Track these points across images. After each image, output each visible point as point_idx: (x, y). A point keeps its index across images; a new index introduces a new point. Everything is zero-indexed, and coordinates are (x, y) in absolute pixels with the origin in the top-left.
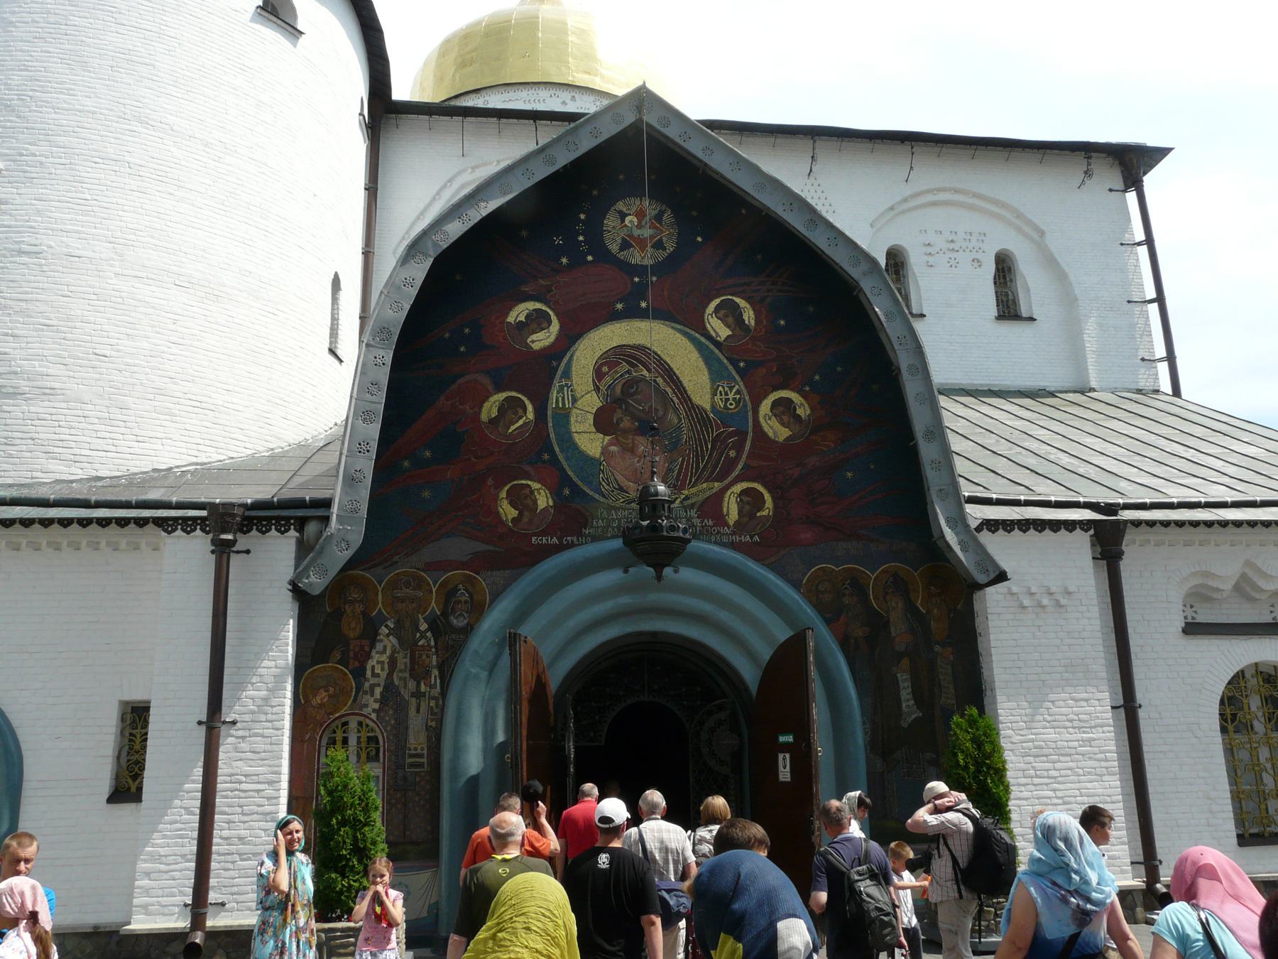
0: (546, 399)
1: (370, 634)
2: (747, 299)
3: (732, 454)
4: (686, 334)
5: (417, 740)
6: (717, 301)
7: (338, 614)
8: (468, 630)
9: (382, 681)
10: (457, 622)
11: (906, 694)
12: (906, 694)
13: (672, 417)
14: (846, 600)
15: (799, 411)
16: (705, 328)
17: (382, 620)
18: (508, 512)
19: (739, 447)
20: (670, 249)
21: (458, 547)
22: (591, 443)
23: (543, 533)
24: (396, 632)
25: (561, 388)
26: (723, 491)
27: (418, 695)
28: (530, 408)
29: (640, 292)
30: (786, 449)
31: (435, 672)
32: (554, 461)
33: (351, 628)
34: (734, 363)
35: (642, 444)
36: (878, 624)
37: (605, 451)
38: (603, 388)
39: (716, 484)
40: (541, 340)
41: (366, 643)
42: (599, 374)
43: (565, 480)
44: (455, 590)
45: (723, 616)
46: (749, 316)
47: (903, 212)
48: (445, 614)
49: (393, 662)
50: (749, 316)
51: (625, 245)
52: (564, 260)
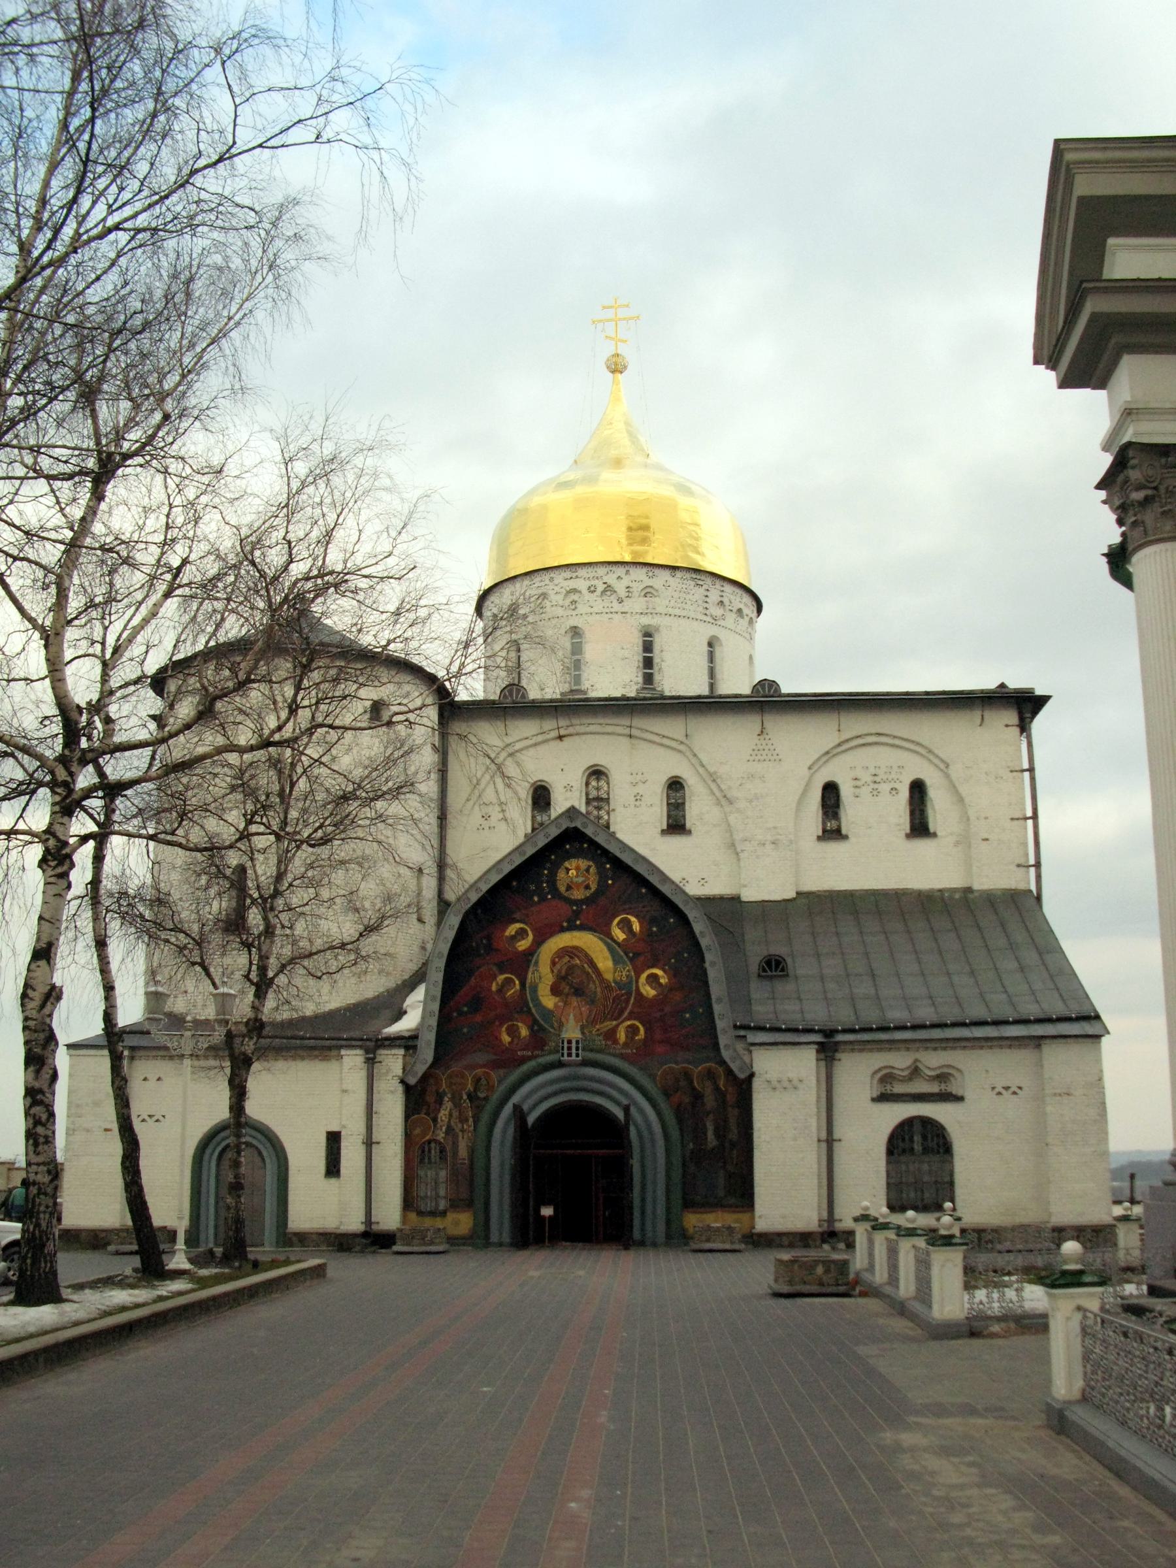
0: (525, 978)
1: (440, 1102)
2: (636, 917)
4: (601, 939)
5: (463, 1152)
7: (423, 1092)
8: (486, 1099)
10: (481, 1095)
11: (710, 1134)
12: (710, 1134)
13: (591, 985)
15: (662, 981)
17: (445, 1093)
18: (506, 1039)
19: (627, 1001)
20: (594, 887)
21: (481, 1058)
22: (549, 1002)
24: (452, 1099)
26: (618, 1026)
27: (463, 1131)
29: (577, 914)
30: (653, 1002)
31: (471, 1120)
33: (430, 1098)
34: (626, 954)
35: (574, 1001)
36: (697, 1097)
37: (556, 1005)
39: (614, 1023)
40: (523, 945)
42: (553, 963)
43: (535, 1021)
44: (479, 1080)
45: (614, 1093)
46: (636, 926)
48: (475, 1090)
49: (451, 1115)
50: (636, 926)
52: (536, 899)
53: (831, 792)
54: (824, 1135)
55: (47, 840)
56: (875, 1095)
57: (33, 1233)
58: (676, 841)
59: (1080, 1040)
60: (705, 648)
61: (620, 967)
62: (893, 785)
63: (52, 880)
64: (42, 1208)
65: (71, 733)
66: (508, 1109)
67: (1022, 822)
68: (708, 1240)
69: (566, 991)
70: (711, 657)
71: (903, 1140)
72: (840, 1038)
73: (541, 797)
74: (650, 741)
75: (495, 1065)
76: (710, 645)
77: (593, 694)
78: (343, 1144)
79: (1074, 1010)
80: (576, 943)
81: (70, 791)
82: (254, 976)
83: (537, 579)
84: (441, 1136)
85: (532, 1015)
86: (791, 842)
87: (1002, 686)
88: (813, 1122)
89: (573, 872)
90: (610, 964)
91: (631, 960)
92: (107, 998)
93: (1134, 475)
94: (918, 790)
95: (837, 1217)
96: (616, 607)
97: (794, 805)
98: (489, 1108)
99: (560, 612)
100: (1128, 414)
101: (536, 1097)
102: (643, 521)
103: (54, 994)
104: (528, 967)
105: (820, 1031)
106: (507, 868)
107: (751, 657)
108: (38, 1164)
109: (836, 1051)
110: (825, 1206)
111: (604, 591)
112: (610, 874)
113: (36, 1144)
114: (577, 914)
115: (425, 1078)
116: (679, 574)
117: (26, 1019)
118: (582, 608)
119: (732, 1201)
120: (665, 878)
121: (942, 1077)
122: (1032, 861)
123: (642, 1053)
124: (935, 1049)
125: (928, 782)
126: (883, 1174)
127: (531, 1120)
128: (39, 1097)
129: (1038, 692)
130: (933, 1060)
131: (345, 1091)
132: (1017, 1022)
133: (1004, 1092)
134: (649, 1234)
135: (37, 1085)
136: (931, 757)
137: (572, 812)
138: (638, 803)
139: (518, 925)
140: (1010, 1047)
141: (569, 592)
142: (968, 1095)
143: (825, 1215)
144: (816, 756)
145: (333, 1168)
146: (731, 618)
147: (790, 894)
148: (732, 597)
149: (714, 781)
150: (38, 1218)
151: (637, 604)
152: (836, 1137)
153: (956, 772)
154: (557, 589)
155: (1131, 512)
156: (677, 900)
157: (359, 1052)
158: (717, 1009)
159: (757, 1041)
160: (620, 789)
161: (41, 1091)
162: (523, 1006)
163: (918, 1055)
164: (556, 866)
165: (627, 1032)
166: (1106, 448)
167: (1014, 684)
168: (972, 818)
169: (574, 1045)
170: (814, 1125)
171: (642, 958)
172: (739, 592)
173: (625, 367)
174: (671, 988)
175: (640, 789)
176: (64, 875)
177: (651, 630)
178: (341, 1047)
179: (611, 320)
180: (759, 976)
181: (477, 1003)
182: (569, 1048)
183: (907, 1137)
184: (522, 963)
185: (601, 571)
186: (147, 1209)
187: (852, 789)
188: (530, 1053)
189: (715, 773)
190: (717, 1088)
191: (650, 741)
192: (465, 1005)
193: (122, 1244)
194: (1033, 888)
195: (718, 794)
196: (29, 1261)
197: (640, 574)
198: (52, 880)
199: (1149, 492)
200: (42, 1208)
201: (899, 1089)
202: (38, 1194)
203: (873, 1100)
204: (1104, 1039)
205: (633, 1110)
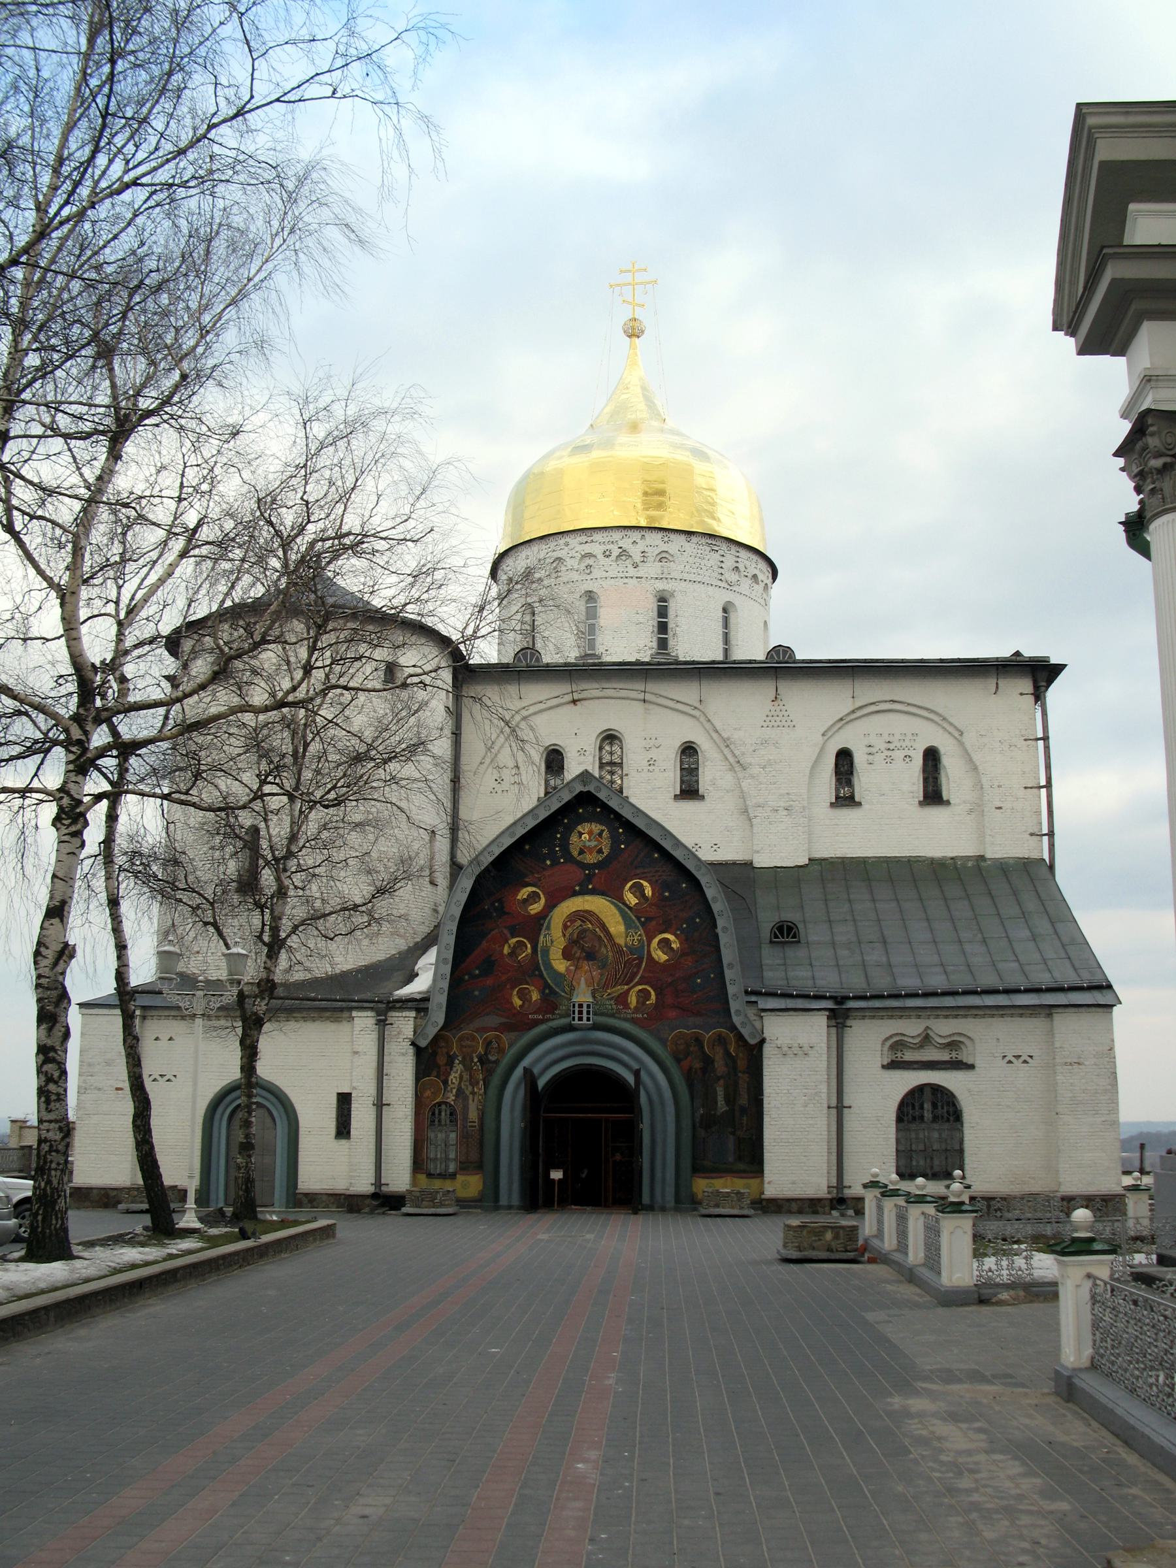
1: (450, 1063)
3: (635, 970)
4: (613, 903)
5: (473, 1115)
6: (631, 883)
7: (435, 1054)
8: (497, 1062)
9: (456, 1086)
10: (492, 1058)
13: (603, 950)
14: (692, 1049)
15: (674, 946)
16: (623, 899)
18: (517, 1002)
19: (639, 966)
20: (606, 851)
21: (493, 1020)
22: (561, 966)
23: (534, 1013)
25: (545, 936)
26: (629, 990)
27: (473, 1093)
28: (529, 946)
29: (589, 878)
30: (664, 967)
31: (481, 1082)
32: (541, 975)
33: (441, 1060)
34: (639, 918)
35: (586, 966)
36: (708, 1061)
37: (567, 969)
38: (567, 935)
40: (535, 908)
41: (448, 1068)
42: (565, 927)
43: (547, 986)
44: (491, 1042)
45: (625, 1058)
46: (648, 891)
47: (852, 720)
48: (486, 1054)
49: (461, 1077)
50: (648, 891)
51: (582, 852)
52: (548, 862)
53: (844, 759)
54: (834, 1102)
55: (62, 798)
56: (885, 1063)
57: (45, 1190)
58: (689, 806)
59: (1090, 1009)
60: (720, 614)
61: (632, 931)
62: (907, 752)
63: (66, 838)
64: (54, 1166)
65: (86, 691)
66: (519, 1072)
67: (1035, 790)
68: (717, 1206)
69: (578, 955)
70: (726, 623)
71: (913, 1108)
72: (851, 1004)
73: (554, 760)
74: (666, 707)
75: (506, 1028)
76: (725, 610)
77: (607, 659)
78: (354, 1106)
79: (1086, 979)
80: (587, 907)
81: (85, 750)
82: (266, 938)
83: (552, 544)
84: (451, 1098)
85: (544, 979)
86: (804, 807)
87: (1017, 654)
88: (823, 1088)
89: (585, 836)
90: (622, 928)
91: (643, 924)
92: (119, 958)
93: (1153, 442)
94: (932, 757)
95: (846, 1183)
96: (632, 571)
97: (808, 772)
98: (500, 1070)
99: (575, 576)
100: (1148, 380)
101: (548, 1059)
102: (661, 486)
103: (66, 952)
104: (541, 930)
105: (831, 998)
106: (520, 832)
107: (765, 622)
108: (50, 1121)
109: (847, 1017)
110: (834, 1172)
111: (619, 556)
112: (622, 838)
113: (48, 1102)
114: (589, 878)
115: (437, 1038)
116: (694, 539)
117: (39, 977)
118: (597, 573)
119: (741, 1166)
120: (678, 843)
121: (953, 1045)
122: (1045, 830)
123: (652, 1018)
124: (946, 1017)
125: (942, 750)
126: (893, 1141)
127: (541, 1083)
128: (52, 1054)
129: (1053, 661)
130: (944, 1028)
131: (356, 1053)
132: (1028, 991)
133: (1013, 1059)
134: (658, 1198)
135: (49, 1042)
136: (945, 725)
137: (585, 776)
138: (651, 768)
139: (531, 889)
140: (1021, 1015)
141: (584, 556)
142: (978, 1063)
143: (834, 1182)
144: (831, 723)
145: (343, 1129)
146: (746, 584)
147: (803, 860)
148: (748, 563)
149: (727, 746)
150: (49, 1175)
151: (652, 569)
152: (846, 1103)
153: (969, 739)
154: (572, 553)
155: (1149, 480)
156: (690, 865)
157: (369, 1013)
158: (729, 974)
159: (769, 1006)
160: (634, 755)
161: (53, 1049)
162: (534, 970)
163: (929, 1023)
164: (569, 829)
165: (638, 996)
166: (1124, 416)
167: (1028, 652)
168: (986, 786)
169: (585, 1009)
170: (824, 1091)
171: (654, 923)
172: (755, 557)
173: (643, 332)
174: (683, 953)
175: (653, 754)
176: (78, 834)
177: (667, 595)
178: (351, 1009)
179: (629, 284)
180: (771, 942)
181: (489, 965)
182: (580, 1012)
183: (917, 1105)
184: (534, 927)
185: (616, 536)
186: (158, 1167)
187: (866, 756)
188: (541, 1017)
189: (728, 739)
190: (727, 1053)
191: (666, 707)
192: (477, 968)
193: (132, 1202)
194: (1046, 857)
195: (732, 760)
196: (40, 1218)
197: (655, 538)
198: (66, 838)
199: (1168, 460)
200: (54, 1166)
201: (909, 1056)
202: (50, 1151)
203: (883, 1067)
204: (1115, 1008)
205: (644, 1075)
